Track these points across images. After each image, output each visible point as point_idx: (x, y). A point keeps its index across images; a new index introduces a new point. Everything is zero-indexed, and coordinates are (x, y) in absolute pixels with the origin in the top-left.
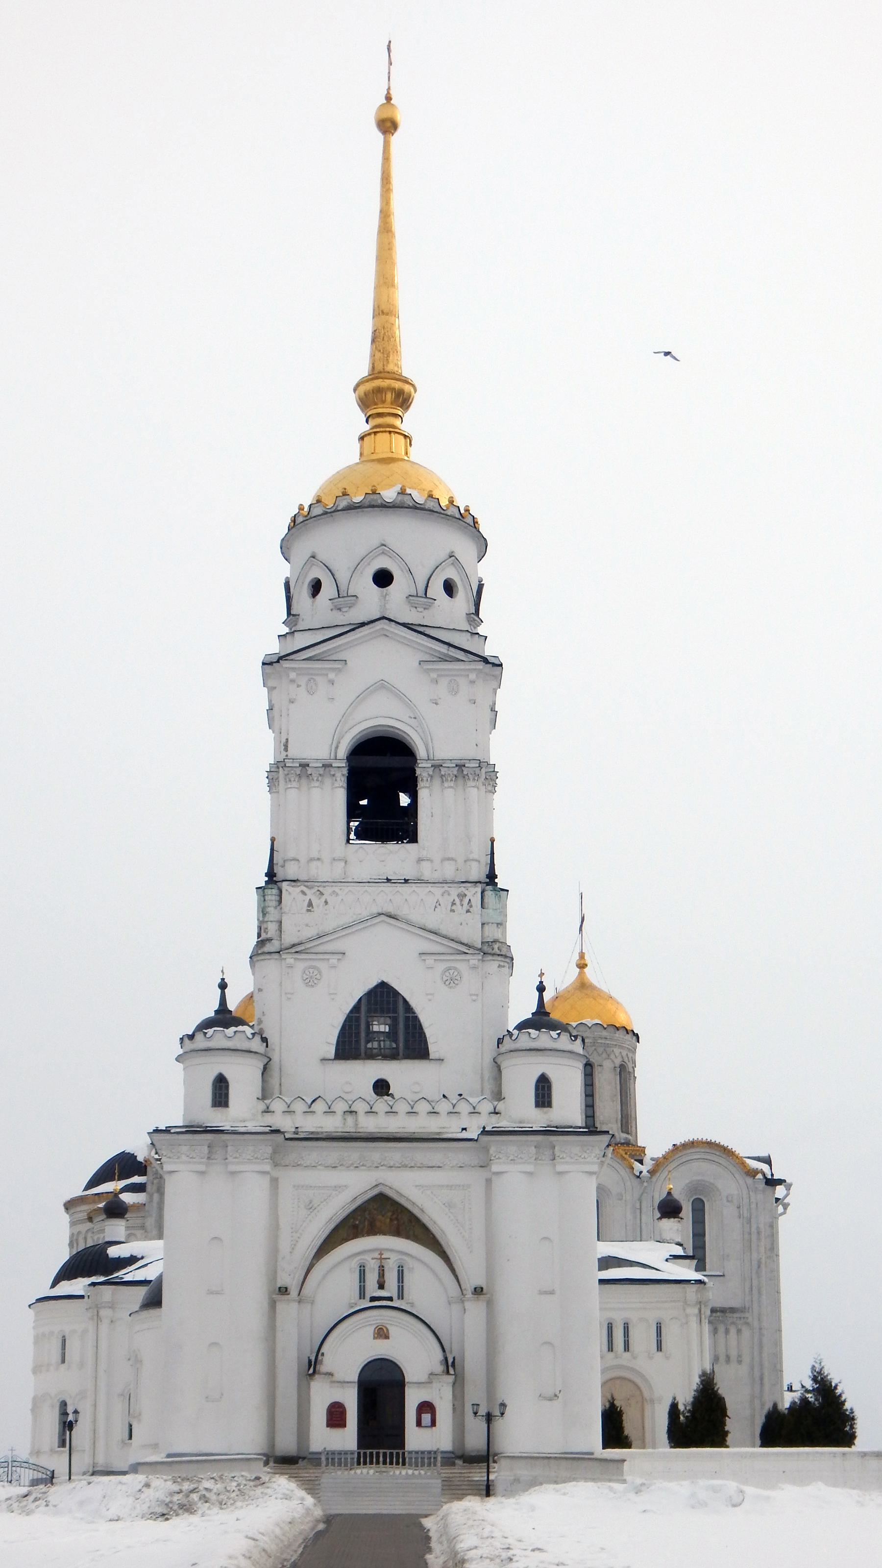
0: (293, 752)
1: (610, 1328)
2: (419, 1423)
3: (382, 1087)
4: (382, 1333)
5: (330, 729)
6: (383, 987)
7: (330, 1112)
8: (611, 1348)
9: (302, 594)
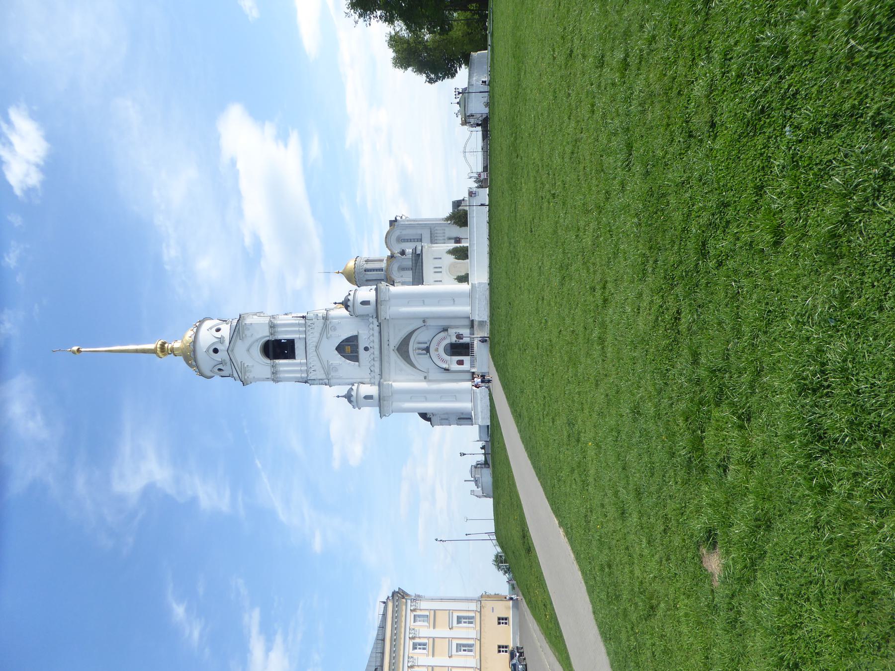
3: (366, 349)
4: (437, 350)
5: (260, 365)
7: (374, 365)
9: (222, 373)
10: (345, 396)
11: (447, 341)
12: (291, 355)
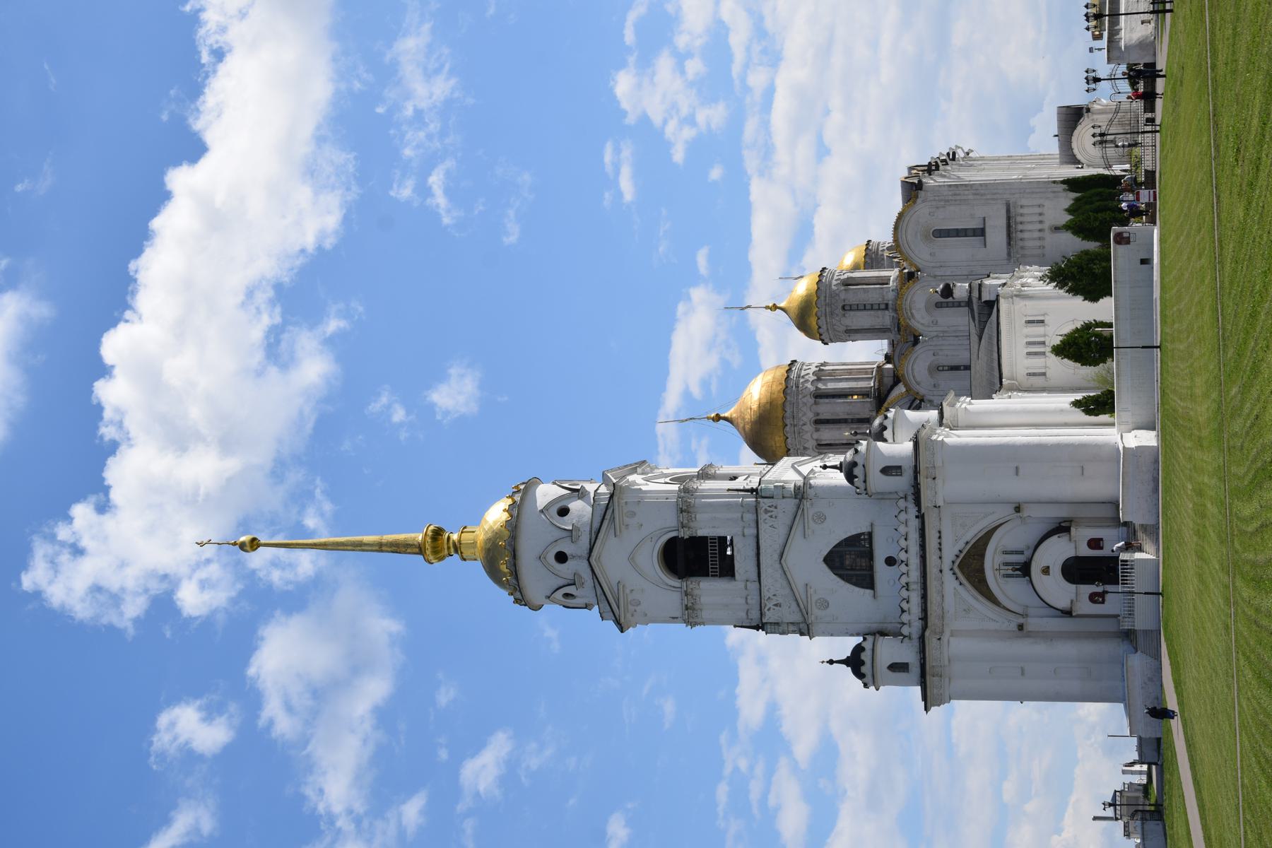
0: (678, 614)
2: (1102, 548)
3: (890, 561)
4: (1046, 571)
10: (845, 662)
11: (1070, 553)
12: (727, 569)
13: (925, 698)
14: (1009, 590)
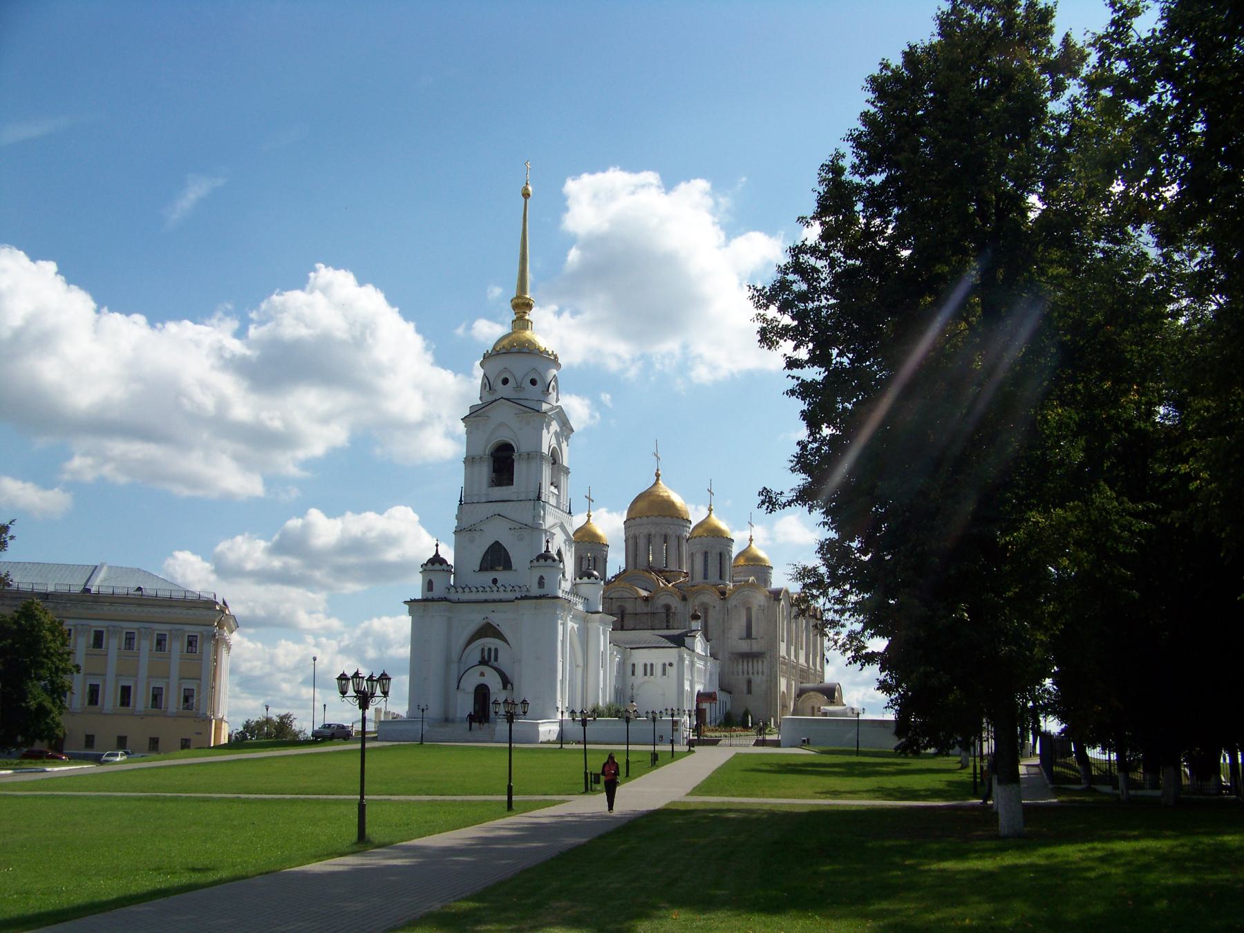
1: (646, 665)
3: (495, 581)
4: (482, 674)
6: (497, 542)
8: (645, 674)
10: (437, 554)
13: (412, 601)
14: (474, 654)
